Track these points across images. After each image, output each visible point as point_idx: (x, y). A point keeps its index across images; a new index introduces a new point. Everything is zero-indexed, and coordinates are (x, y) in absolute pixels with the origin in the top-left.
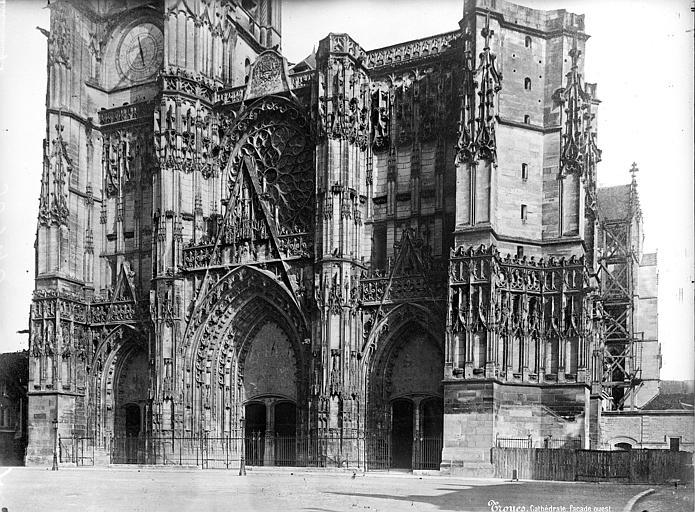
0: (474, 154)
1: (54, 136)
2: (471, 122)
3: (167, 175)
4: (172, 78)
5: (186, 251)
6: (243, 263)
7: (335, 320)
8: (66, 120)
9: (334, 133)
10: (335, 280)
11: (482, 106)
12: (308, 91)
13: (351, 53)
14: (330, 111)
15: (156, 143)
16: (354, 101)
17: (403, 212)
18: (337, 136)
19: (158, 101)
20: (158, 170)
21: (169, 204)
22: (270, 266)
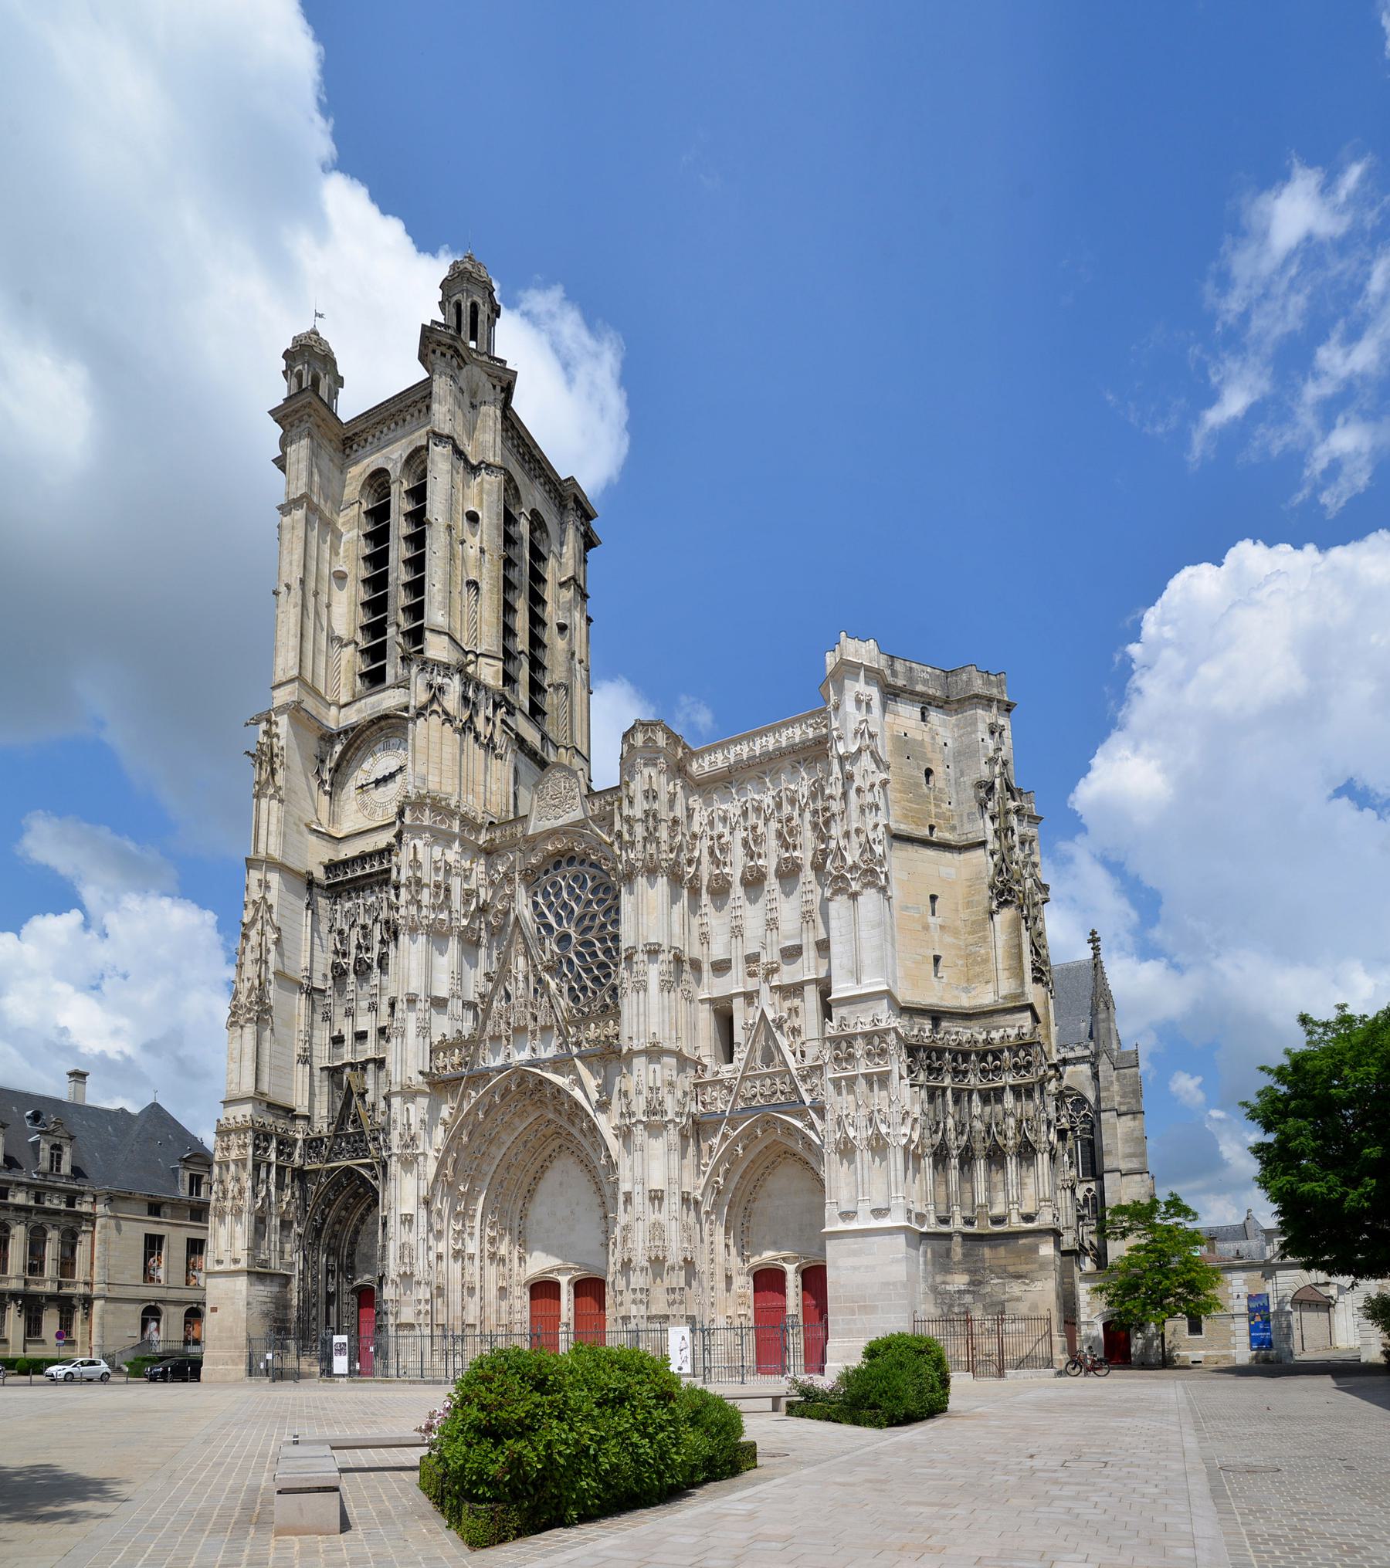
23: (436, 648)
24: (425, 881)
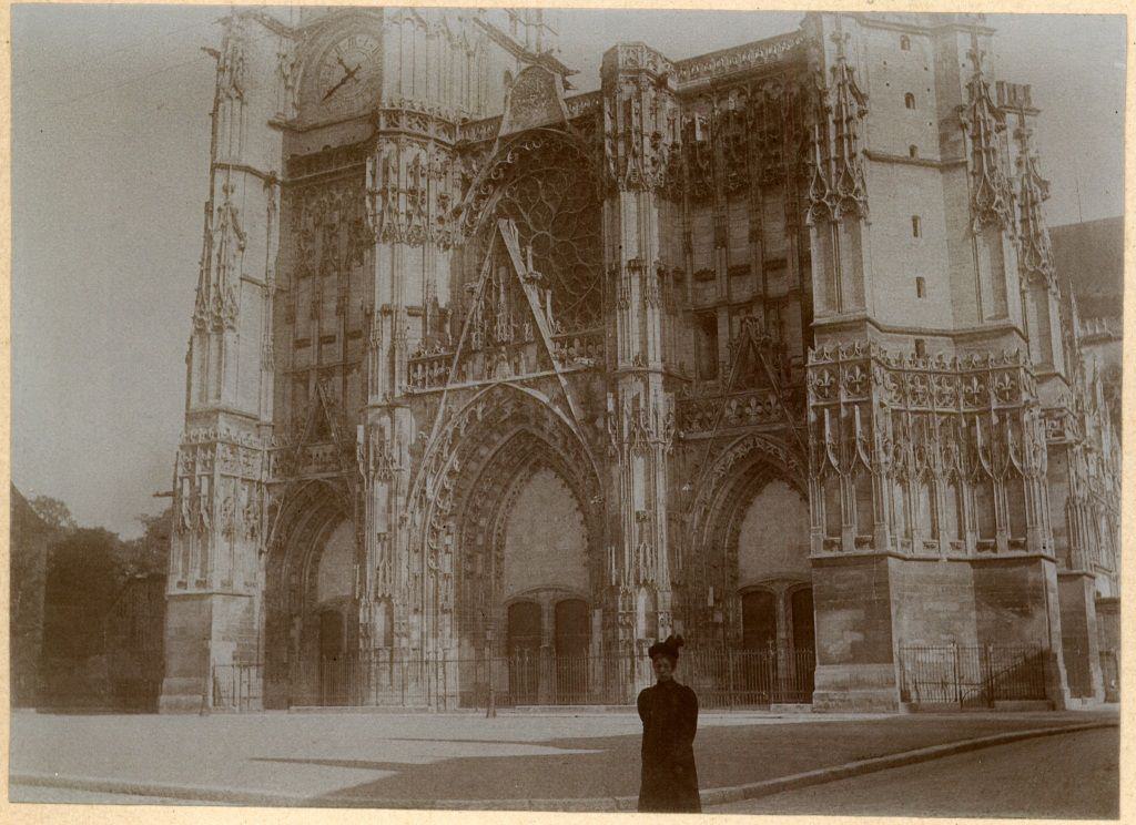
0: (834, 208)
1: (219, 201)
2: (826, 162)
3: (382, 250)
4: (394, 115)
5: (413, 364)
6: (499, 379)
7: (639, 464)
8: (238, 179)
9: (629, 183)
10: (636, 400)
11: (840, 139)
12: (588, 122)
13: (651, 68)
14: (621, 152)
15: (368, 205)
16: (657, 136)
17: (743, 291)
18: (630, 186)
20: (371, 244)
21: (382, 297)
24: (403, 186)
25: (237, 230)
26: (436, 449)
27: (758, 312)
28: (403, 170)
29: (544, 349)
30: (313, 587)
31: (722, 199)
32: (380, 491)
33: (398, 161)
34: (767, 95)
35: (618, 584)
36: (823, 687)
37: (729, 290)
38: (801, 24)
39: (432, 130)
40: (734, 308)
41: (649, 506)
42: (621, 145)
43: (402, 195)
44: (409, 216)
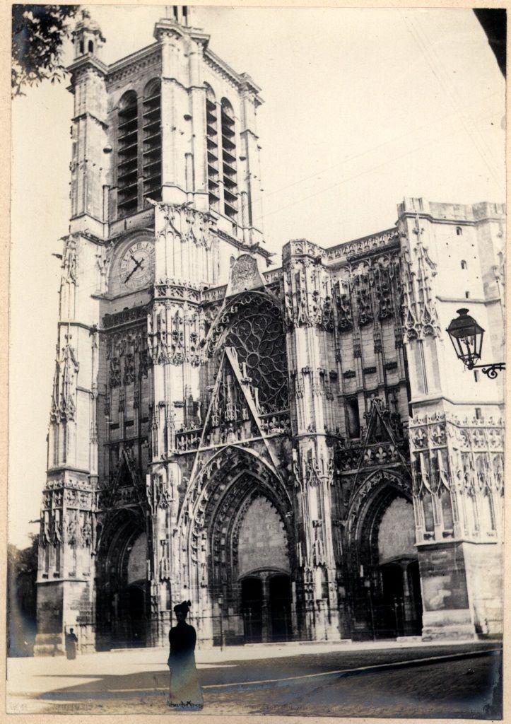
0: (420, 332)
1: (63, 344)
2: (414, 305)
3: (158, 369)
4: (163, 288)
5: (178, 436)
6: (228, 443)
7: (313, 491)
8: (73, 330)
9: (300, 322)
10: (310, 453)
11: (421, 290)
12: (276, 286)
13: (311, 253)
14: (295, 304)
15: (149, 342)
16: (316, 293)
17: (372, 383)
18: (301, 324)
19: (151, 305)
20: (152, 365)
21: (159, 397)
22: (251, 445)
23: (169, 195)
24: (169, 331)
25: (73, 360)
26: (193, 487)
27: (382, 396)
28: (169, 322)
29: (254, 424)
30: (126, 574)
31: (357, 329)
32: (161, 514)
33: (166, 315)
34: (381, 265)
35: (304, 565)
36: (428, 626)
37: (364, 382)
38: (396, 224)
39: (186, 295)
40: (367, 394)
41: (320, 517)
42: (295, 300)
43: (169, 336)
44: (173, 347)
